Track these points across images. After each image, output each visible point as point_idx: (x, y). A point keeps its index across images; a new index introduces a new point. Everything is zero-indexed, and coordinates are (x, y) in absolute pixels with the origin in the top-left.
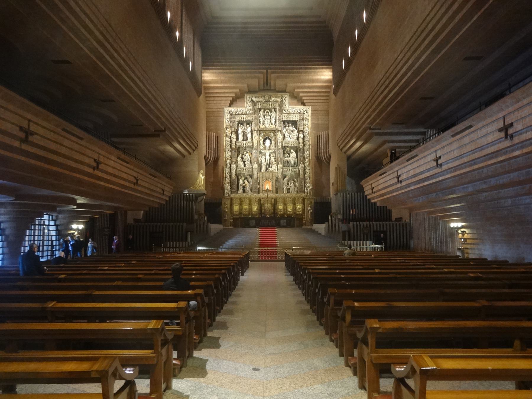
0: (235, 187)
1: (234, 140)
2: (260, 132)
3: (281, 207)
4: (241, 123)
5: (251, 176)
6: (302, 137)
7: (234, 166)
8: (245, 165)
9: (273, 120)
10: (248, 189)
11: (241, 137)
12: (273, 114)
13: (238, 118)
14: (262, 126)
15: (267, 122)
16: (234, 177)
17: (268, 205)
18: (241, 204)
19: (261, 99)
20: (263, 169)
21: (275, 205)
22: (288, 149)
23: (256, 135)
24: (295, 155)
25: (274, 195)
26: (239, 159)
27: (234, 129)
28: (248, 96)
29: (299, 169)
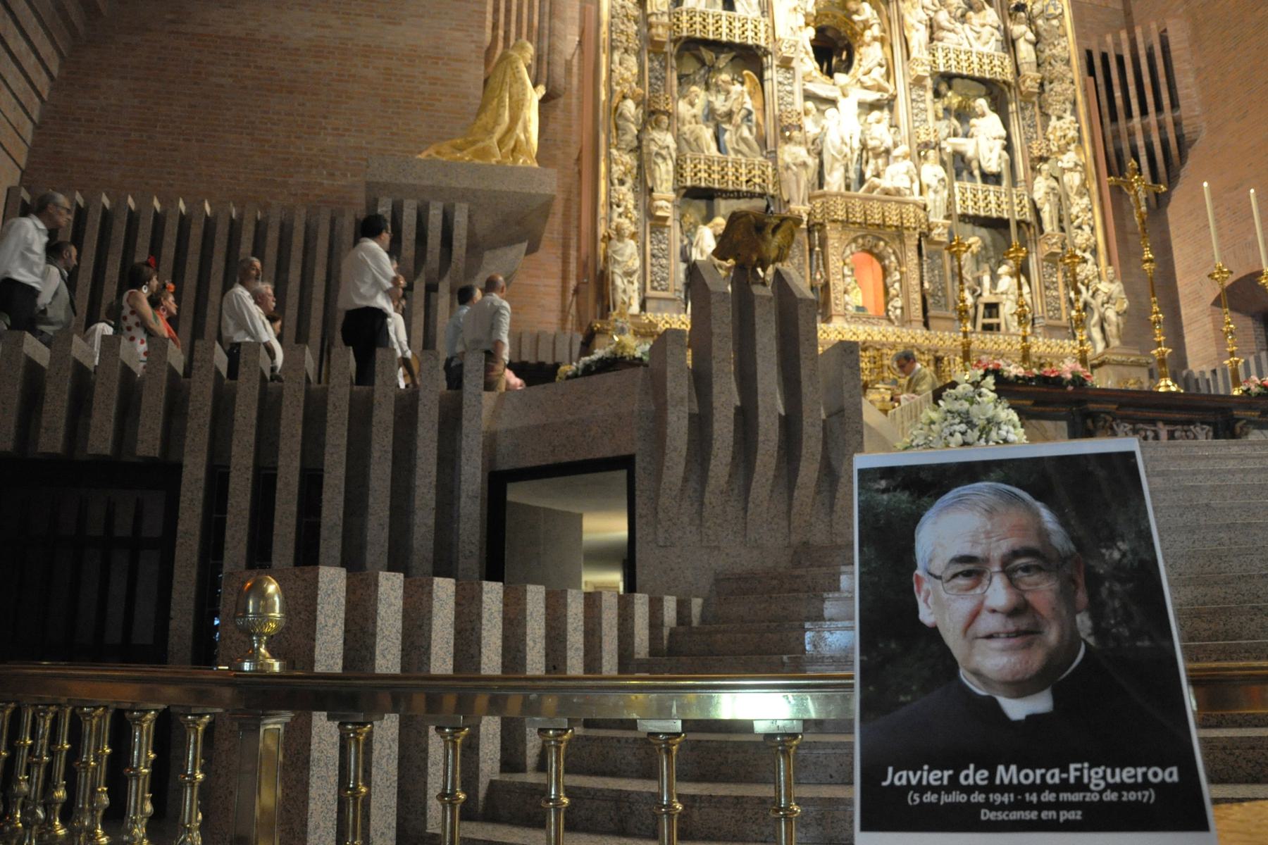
6: (1031, 36)
22: (953, 99)
24: (1003, 133)
25: (915, 335)
29: (1034, 203)
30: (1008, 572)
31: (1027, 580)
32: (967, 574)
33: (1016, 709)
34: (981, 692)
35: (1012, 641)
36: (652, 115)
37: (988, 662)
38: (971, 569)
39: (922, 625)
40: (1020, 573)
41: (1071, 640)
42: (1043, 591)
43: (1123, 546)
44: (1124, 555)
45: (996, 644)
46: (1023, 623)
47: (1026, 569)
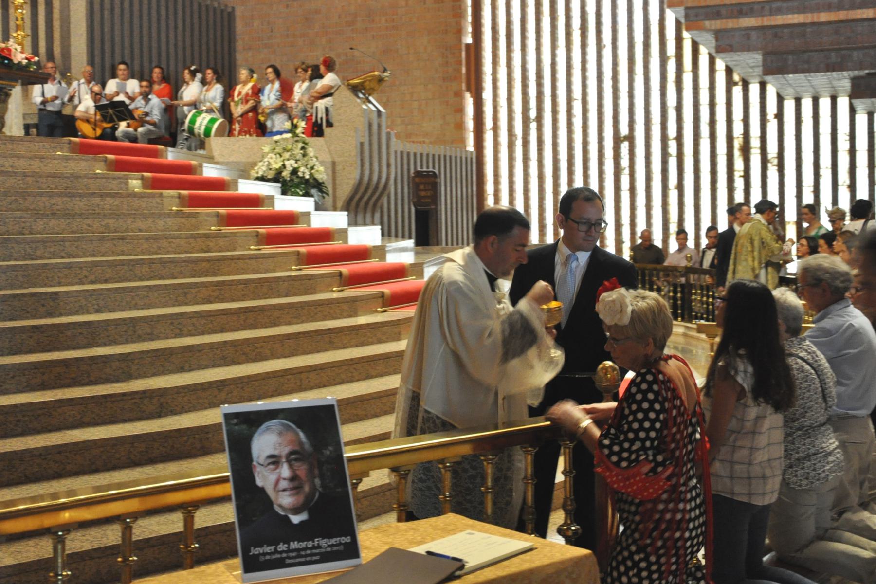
30: (289, 461)
31: (296, 465)
32: (273, 463)
33: (296, 519)
34: (283, 514)
35: (292, 492)
37: (285, 500)
38: (274, 461)
39: (257, 487)
40: (293, 462)
41: (313, 489)
42: (302, 470)
43: (331, 448)
44: (331, 452)
45: (287, 493)
46: (296, 483)
47: (296, 460)
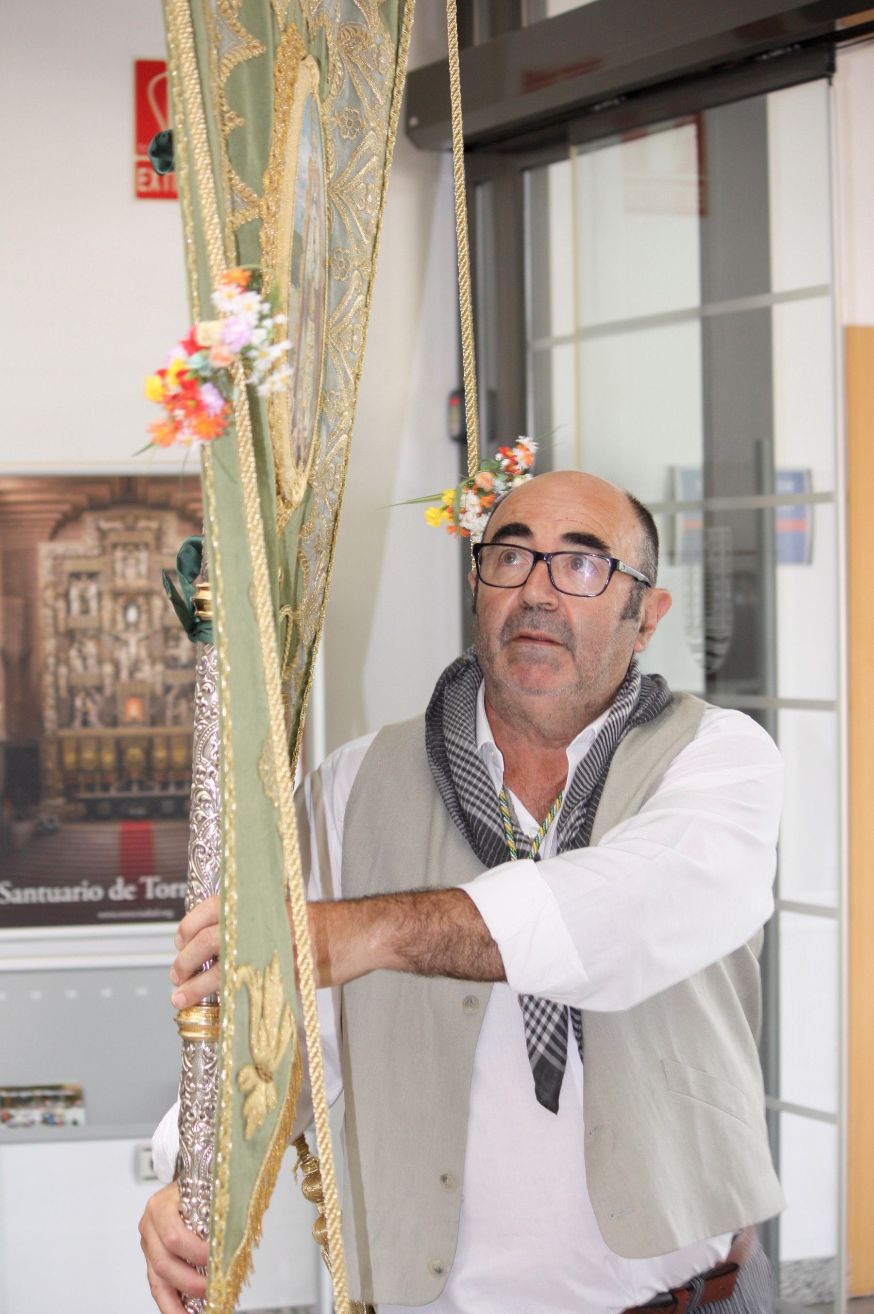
0: (67, 715)
1: (62, 615)
2: (116, 594)
3: (160, 754)
4: (76, 576)
5: (100, 689)
7: (63, 670)
8: (85, 667)
9: (143, 568)
10: (93, 718)
11: (76, 606)
12: (143, 555)
13: (69, 566)
14: (120, 583)
15: (131, 573)
16: (64, 693)
17: (135, 753)
18: (78, 751)
19: (117, 525)
20: (124, 675)
21: (148, 752)
23: (107, 603)
26: (73, 653)
27: (61, 589)
28: (89, 519)
36: (58, 662)
